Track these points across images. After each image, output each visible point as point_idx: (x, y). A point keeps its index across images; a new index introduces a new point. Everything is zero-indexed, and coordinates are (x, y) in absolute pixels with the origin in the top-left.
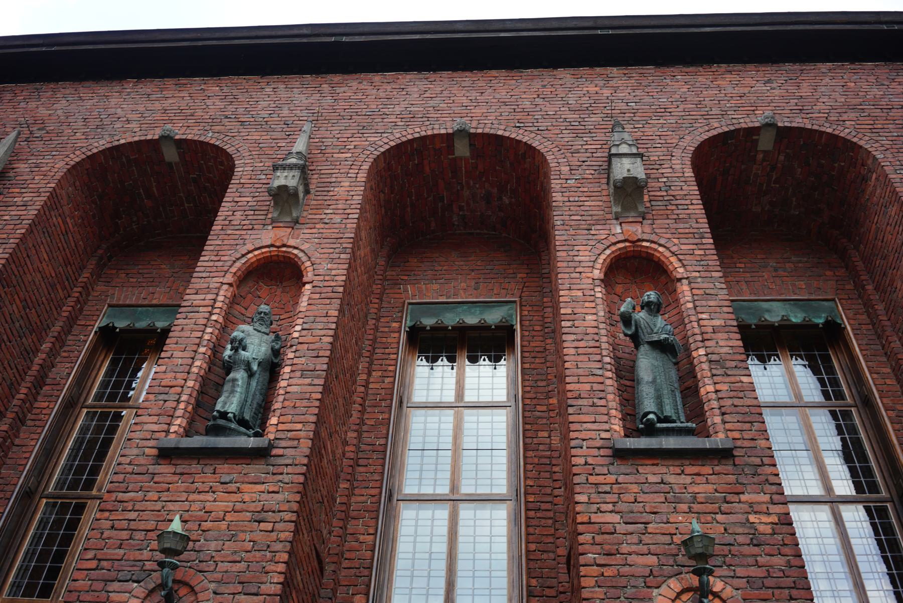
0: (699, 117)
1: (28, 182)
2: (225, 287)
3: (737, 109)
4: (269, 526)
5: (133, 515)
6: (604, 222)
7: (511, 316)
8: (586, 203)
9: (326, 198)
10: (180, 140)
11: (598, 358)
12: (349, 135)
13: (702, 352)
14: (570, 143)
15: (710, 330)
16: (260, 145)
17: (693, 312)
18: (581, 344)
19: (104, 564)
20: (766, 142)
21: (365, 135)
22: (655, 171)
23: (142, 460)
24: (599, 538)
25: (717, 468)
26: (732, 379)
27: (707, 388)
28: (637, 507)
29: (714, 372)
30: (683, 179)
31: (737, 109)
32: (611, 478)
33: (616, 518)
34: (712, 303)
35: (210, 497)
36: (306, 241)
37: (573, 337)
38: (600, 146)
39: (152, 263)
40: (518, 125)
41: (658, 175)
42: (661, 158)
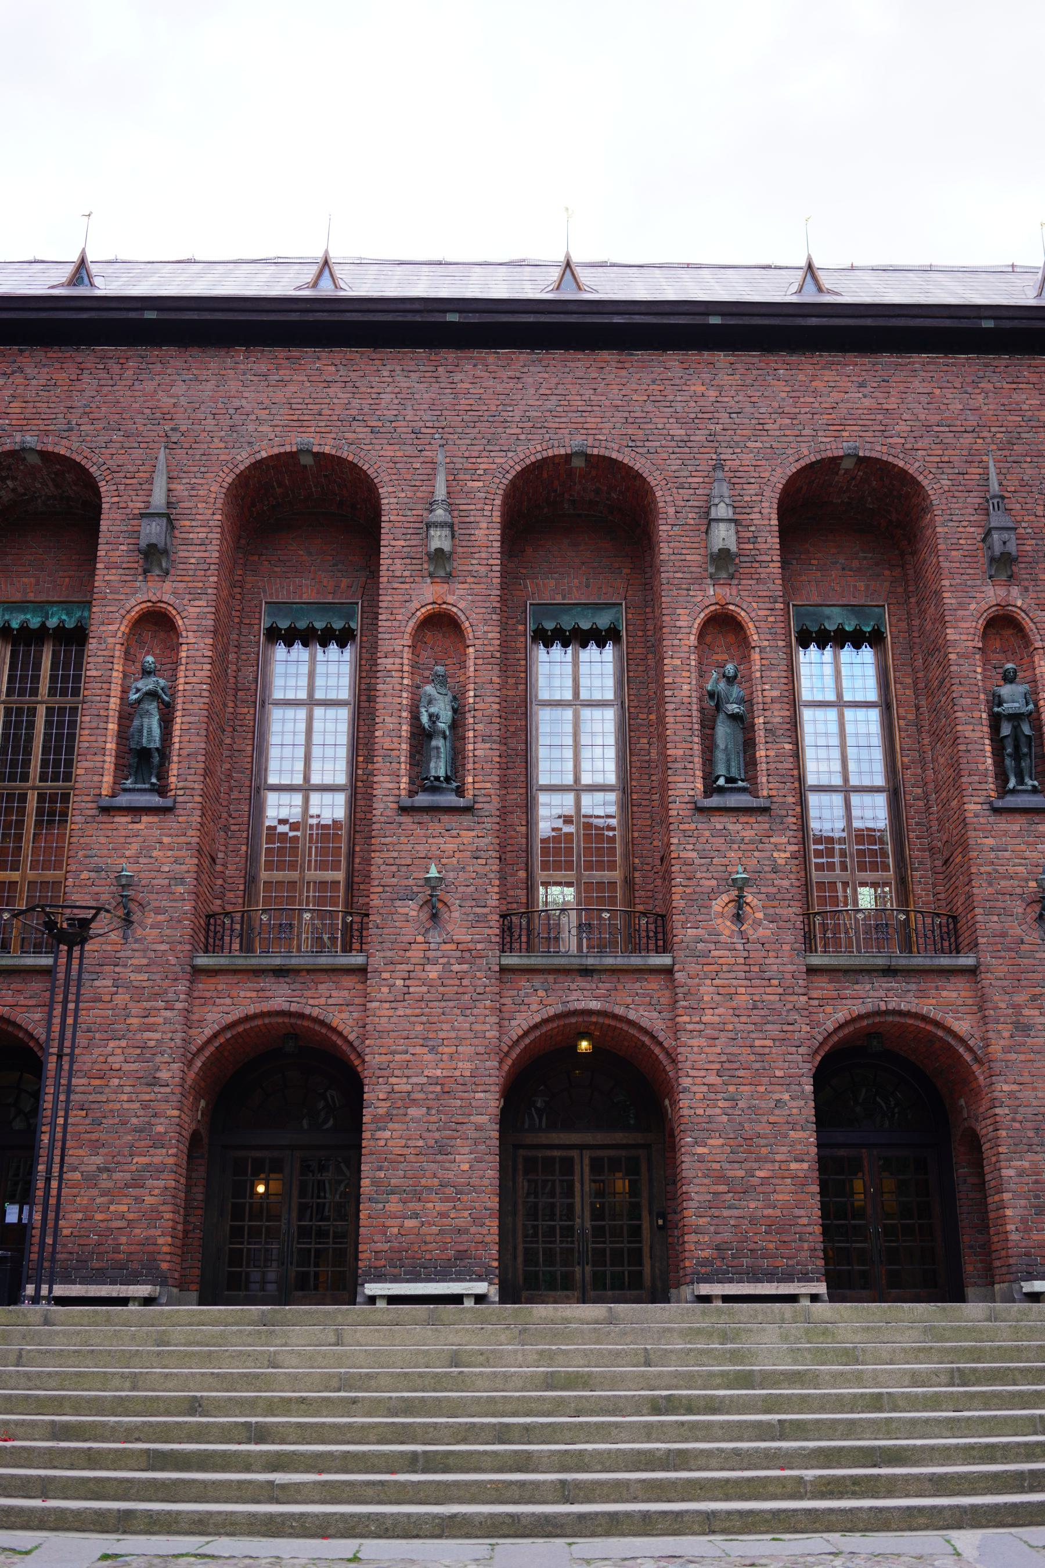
0: (791, 439)
1: (194, 511)
2: (406, 649)
3: (826, 427)
4: (483, 862)
5: (395, 854)
6: (700, 581)
7: (617, 620)
8: (688, 557)
9: (470, 544)
10: (318, 453)
11: (689, 726)
12: (476, 454)
13: (761, 720)
14: (677, 474)
15: (769, 700)
16: (398, 466)
17: (759, 681)
18: (679, 713)
19: (387, 889)
20: (848, 464)
21: (492, 454)
22: (746, 516)
23: (389, 813)
24: (684, 868)
25: (759, 819)
26: (779, 746)
27: (761, 753)
28: (708, 846)
29: (768, 740)
30: (768, 528)
31: (826, 427)
32: (693, 826)
33: (694, 854)
34: (774, 674)
35: (441, 840)
36: (461, 598)
37: (673, 706)
38: (701, 480)
40: (630, 444)
41: (748, 522)
42: (754, 498)
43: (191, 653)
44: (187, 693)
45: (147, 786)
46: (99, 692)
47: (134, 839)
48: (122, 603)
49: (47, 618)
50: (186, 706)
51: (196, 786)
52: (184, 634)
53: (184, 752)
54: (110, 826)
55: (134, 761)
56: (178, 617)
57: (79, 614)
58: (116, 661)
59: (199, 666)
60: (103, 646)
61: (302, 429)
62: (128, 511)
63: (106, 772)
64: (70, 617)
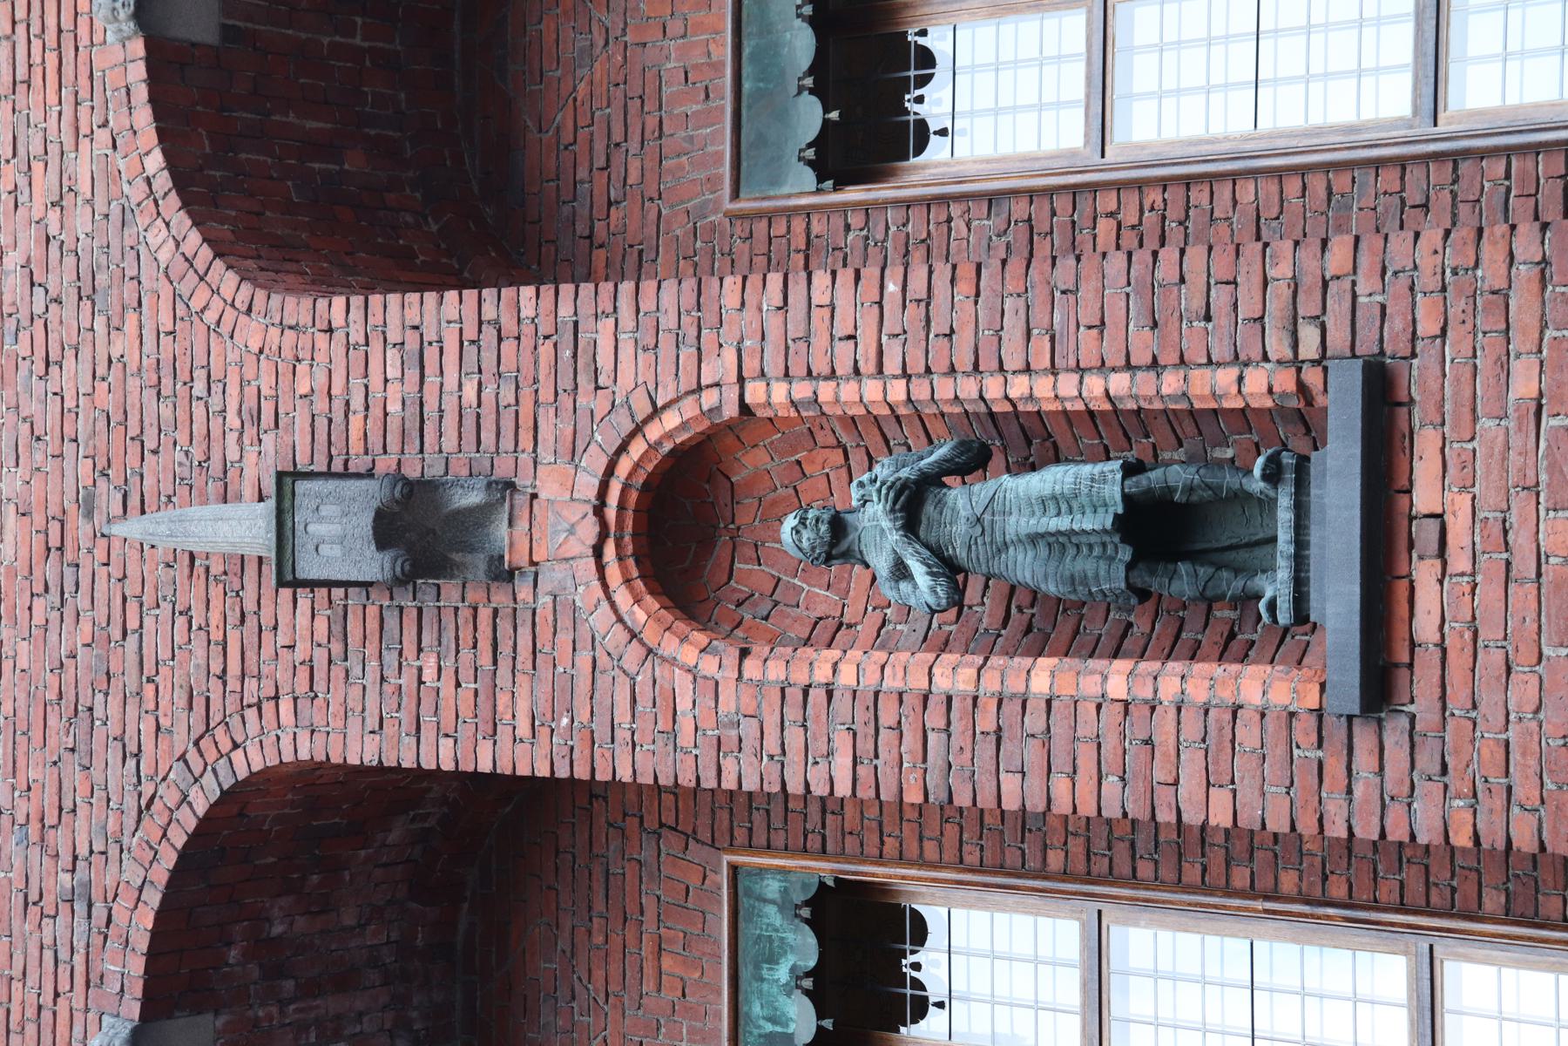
1: (320, 405)
39: (567, 137)
43: (774, 366)
45: (1285, 501)
46: (911, 741)
47: (1521, 539)
48: (603, 661)
50: (964, 360)
51: (1281, 271)
53: (1143, 345)
55: (1184, 581)
57: (772, 915)
58: (800, 677)
60: (749, 729)
61: (83, 31)
62: (320, 656)
64: (785, 948)
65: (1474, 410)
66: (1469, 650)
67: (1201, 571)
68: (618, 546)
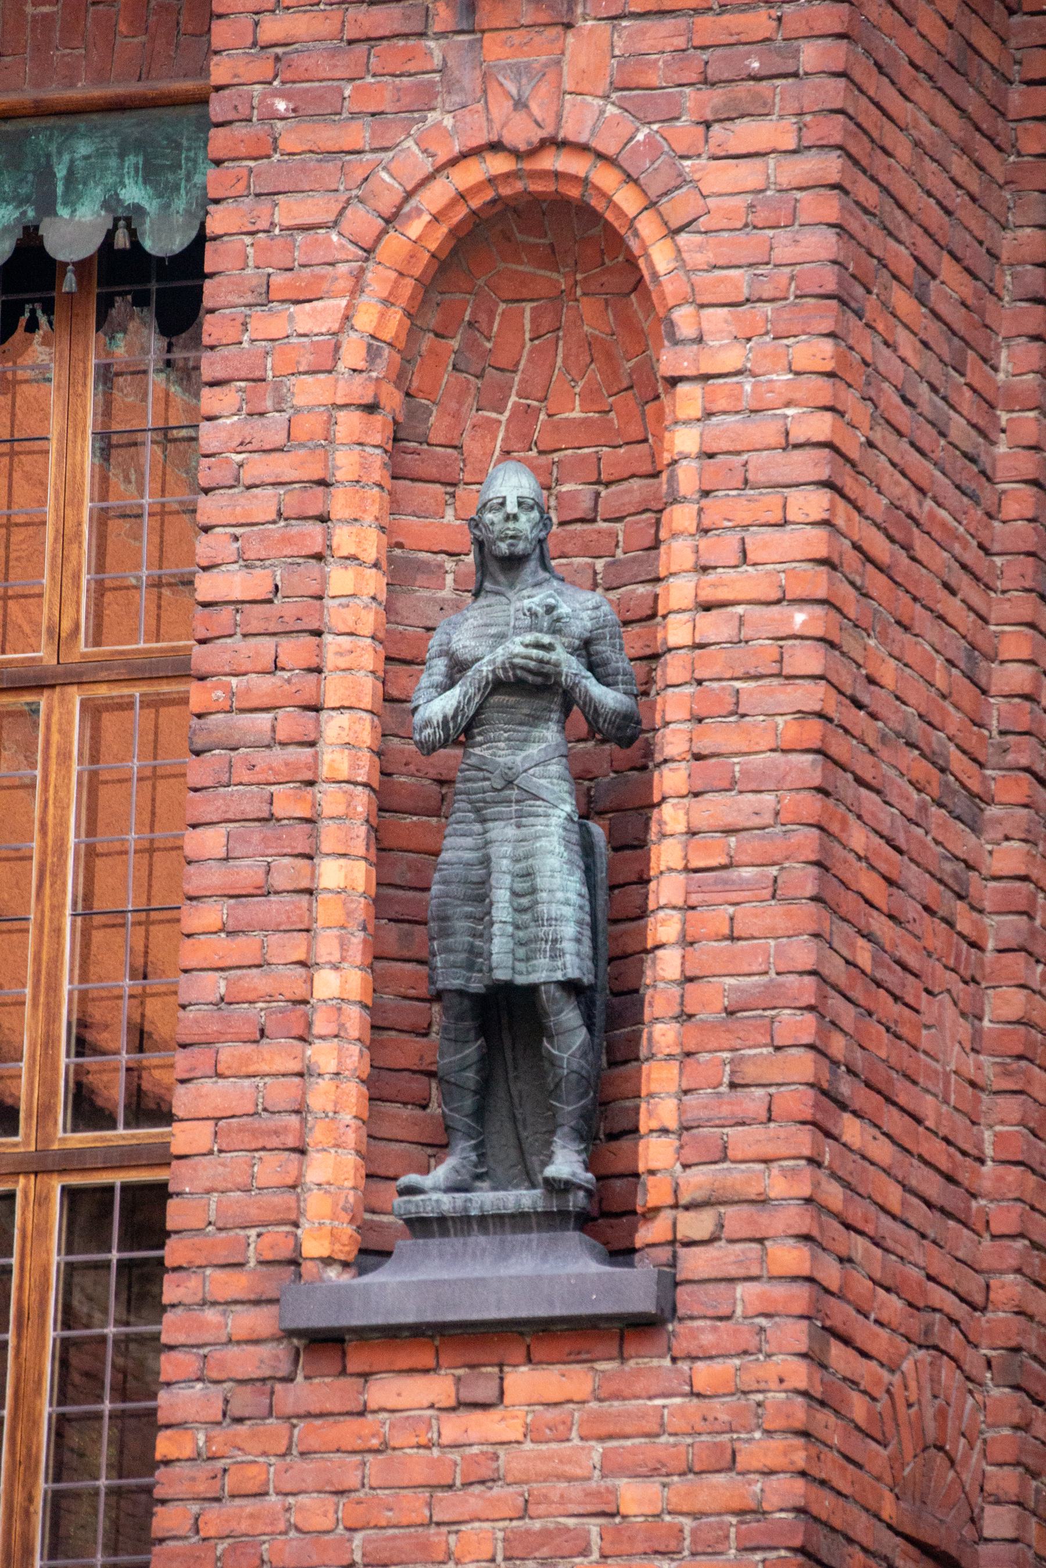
44: (710, 665)
46: (263, 686)
47: (474, 1500)
48: (359, 167)
49: (48, 208)
51: (776, 1184)
52: (684, 319)
54: (348, 1431)
56: (648, 227)
58: (339, 504)
59: (768, 506)
60: (276, 423)
63: (317, 1136)
64: (166, 192)
65: (611, 1437)
66: (359, 1444)
67: (470, 1074)
68: (507, 176)
